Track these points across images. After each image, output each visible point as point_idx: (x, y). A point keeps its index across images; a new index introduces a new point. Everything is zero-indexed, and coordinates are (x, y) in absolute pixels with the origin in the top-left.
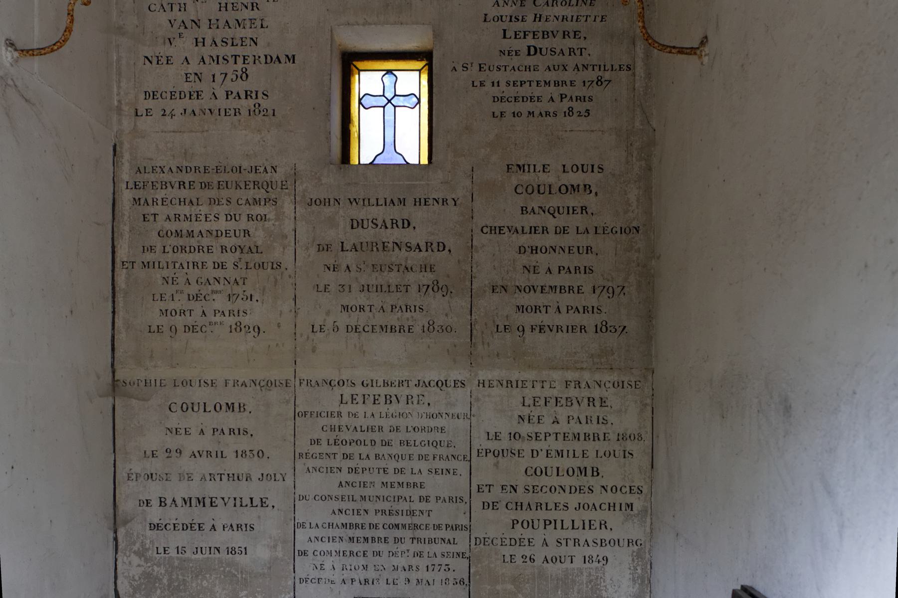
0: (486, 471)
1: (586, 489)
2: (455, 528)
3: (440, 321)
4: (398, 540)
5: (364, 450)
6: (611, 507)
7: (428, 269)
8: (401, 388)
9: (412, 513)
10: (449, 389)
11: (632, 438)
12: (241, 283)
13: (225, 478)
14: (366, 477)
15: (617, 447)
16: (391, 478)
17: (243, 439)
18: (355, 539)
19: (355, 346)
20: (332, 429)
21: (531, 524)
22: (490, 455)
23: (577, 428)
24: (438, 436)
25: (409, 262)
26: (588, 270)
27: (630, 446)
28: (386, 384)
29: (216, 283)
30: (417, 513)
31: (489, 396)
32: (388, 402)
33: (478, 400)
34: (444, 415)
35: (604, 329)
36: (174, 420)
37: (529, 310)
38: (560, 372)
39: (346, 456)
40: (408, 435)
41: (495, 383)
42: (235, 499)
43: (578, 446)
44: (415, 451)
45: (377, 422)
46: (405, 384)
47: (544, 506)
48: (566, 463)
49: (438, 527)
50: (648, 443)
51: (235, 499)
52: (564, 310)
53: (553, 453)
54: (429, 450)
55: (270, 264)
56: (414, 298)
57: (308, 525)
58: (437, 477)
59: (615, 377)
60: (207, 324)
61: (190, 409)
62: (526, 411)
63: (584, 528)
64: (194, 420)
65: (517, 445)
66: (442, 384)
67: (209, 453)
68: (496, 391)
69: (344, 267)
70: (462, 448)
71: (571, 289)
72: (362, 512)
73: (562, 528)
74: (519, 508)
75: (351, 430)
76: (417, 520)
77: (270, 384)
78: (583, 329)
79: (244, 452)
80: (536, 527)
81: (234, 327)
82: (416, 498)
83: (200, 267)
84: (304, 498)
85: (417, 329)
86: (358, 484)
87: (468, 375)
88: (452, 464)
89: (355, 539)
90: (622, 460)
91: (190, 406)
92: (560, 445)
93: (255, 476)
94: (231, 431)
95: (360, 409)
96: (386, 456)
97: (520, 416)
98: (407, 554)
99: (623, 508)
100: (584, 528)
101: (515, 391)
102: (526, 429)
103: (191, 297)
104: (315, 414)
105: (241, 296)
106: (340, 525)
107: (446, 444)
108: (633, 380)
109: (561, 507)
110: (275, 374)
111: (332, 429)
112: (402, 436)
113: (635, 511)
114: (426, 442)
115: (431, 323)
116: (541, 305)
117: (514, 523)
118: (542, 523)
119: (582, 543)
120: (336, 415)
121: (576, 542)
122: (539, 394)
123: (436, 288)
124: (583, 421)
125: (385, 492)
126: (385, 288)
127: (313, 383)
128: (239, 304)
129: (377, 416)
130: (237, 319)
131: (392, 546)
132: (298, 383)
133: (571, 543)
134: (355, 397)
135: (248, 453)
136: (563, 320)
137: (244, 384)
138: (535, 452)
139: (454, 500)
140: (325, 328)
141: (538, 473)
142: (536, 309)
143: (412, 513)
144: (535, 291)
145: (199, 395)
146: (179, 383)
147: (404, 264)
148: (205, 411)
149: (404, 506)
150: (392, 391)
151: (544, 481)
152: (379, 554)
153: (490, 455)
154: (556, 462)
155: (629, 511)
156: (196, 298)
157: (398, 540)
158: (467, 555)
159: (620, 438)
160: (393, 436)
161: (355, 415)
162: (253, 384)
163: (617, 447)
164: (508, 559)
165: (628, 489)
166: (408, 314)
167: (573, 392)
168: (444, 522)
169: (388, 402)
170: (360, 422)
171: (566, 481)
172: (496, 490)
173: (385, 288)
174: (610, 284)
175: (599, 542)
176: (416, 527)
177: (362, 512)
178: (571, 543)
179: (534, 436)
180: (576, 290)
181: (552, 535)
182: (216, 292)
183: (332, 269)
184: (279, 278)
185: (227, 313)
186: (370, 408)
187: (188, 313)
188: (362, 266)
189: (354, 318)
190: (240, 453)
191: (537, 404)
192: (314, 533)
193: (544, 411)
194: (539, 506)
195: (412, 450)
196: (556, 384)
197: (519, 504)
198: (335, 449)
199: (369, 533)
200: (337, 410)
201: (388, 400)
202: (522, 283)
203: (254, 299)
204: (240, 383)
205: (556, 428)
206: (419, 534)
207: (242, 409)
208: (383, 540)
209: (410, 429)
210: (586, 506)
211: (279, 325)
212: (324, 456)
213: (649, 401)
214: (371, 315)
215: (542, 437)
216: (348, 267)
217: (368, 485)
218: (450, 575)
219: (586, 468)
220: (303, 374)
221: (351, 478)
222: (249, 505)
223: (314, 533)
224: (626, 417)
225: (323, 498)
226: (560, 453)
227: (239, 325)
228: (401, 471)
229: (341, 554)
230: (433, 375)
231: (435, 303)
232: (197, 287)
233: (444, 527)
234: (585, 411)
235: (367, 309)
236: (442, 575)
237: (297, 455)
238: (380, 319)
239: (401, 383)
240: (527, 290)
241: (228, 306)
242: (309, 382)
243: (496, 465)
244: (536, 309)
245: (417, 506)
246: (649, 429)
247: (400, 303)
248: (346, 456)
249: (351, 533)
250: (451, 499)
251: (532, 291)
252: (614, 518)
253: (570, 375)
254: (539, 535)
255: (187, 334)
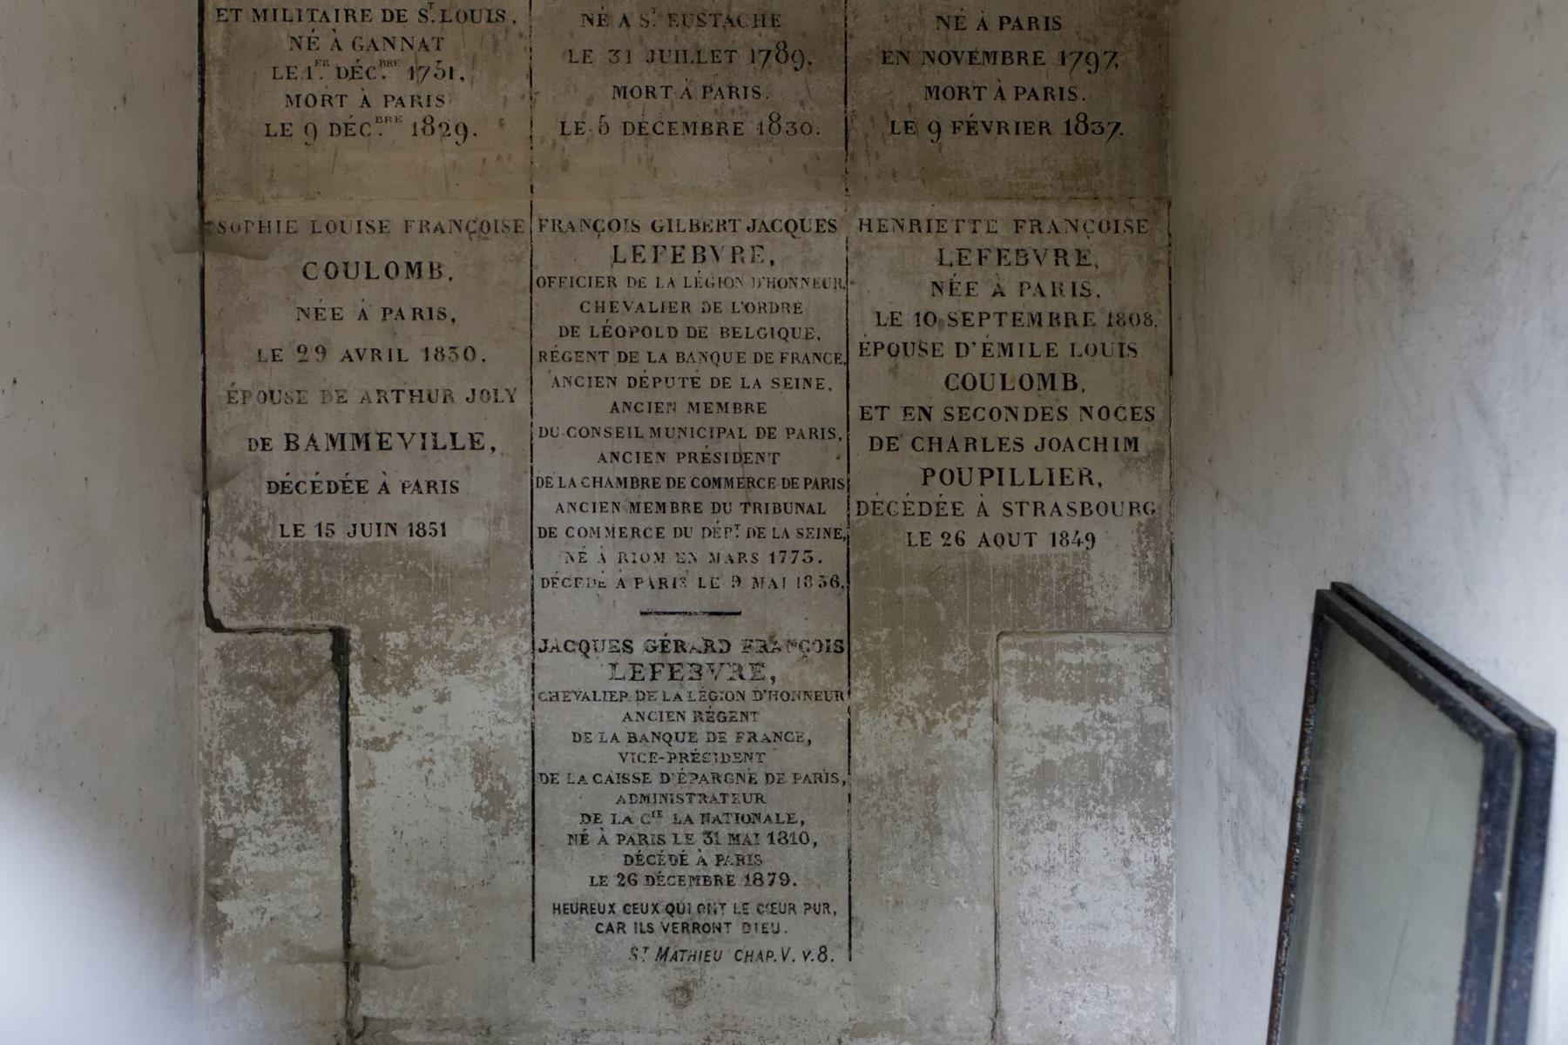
0: (873, 381)
1: (1055, 414)
2: (822, 484)
3: (791, 113)
4: (718, 508)
5: (656, 346)
6: (1100, 444)
7: (768, 23)
8: (722, 234)
9: (743, 458)
10: (808, 236)
11: (1135, 321)
12: (432, 46)
13: (405, 397)
14: (661, 394)
15: (1109, 338)
16: (705, 395)
17: (439, 326)
18: (642, 507)
19: (639, 160)
20: (599, 308)
21: (957, 477)
22: (883, 353)
23: (1036, 305)
24: (790, 320)
25: (734, 9)
26: (1051, 24)
27: (1130, 335)
28: (694, 226)
29: (388, 46)
30: (753, 458)
31: (879, 247)
32: (699, 259)
33: (859, 254)
34: (799, 282)
35: (1081, 128)
36: (314, 293)
37: (949, 95)
38: (1006, 205)
39: (624, 357)
40: (735, 317)
41: (890, 225)
42: (423, 435)
43: (1040, 336)
44: (749, 347)
45: (678, 295)
46: (729, 226)
47: (979, 445)
48: (1019, 366)
49: (791, 483)
50: (1163, 330)
51: (423, 435)
52: (1010, 94)
53: (996, 349)
54: (775, 346)
55: (485, 14)
56: (744, 72)
57: (556, 482)
58: (788, 392)
59: (1101, 213)
60: (373, 122)
61: (341, 274)
62: (946, 274)
63: (1051, 484)
64: (350, 295)
65: (930, 335)
66: (794, 227)
67: (377, 354)
68: (890, 239)
69: (618, 18)
70: (832, 342)
71: (1022, 57)
72: (654, 457)
73: (1013, 483)
74: (935, 448)
75: (633, 309)
76: (752, 471)
77: (487, 228)
78: (1044, 127)
79: (439, 351)
80: (965, 481)
81: (420, 125)
82: (750, 431)
83: (359, 17)
84: (549, 432)
85: (750, 128)
86: (646, 407)
87: (841, 210)
88: (815, 370)
89: (642, 507)
90: (1118, 360)
91: (341, 268)
92: (1006, 334)
93: (461, 393)
94: (417, 313)
95: (648, 271)
96: (696, 356)
97: (934, 283)
98: (734, 532)
99: (1121, 447)
100: (1051, 484)
101: (927, 239)
102: (944, 305)
103: (343, 73)
104: (568, 282)
105: (433, 70)
106: (614, 481)
107: (803, 334)
108: (1135, 218)
109: (1011, 445)
110: (495, 211)
111: (599, 308)
112: (727, 320)
113: (1142, 452)
114: (768, 331)
115: (774, 117)
116: (970, 85)
117: (927, 474)
118: (976, 473)
119: (1048, 509)
120: (605, 282)
121: (1038, 508)
122: (967, 244)
123: (782, 56)
124: (1048, 290)
125: (695, 421)
126: (692, 56)
127: (564, 226)
128: (431, 86)
129: (679, 283)
130: (425, 111)
131: (707, 518)
132: (536, 226)
133: (1029, 509)
134: (639, 249)
135: (447, 352)
136: (1011, 111)
137: (439, 229)
138: (963, 348)
139: (819, 434)
140: (585, 128)
141: (969, 384)
142: (961, 93)
143: (743, 458)
144: (959, 61)
145: (358, 247)
146: (320, 226)
147: (724, 13)
148: (368, 277)
149: (729, 445)
150: (707, 239)
151: (979, 398)
152: (684, 532)
153: (883, 353)
154: (997, 365)
155: (1131, 451)
156: (352, 73)
157: (718, 508)
158: (843, 533)
159: (1114, 321)
160: (706, 320)
161: (639, 283)
162: (455, 229)
163: (1109, 338)
164: (916, 540)
165: (1128, 413)
166: (734, 102)
167: (1029, 241)
168: (801, 473)
169: (699, 259)
170: (649, 294)
171: (1018, 399)
172: (895, 415)
173: (692, 56)
174: (1092, 49)
175: (1078, 507)
176: (752, 483)
177: (654, 457)
178: (1029, 509)
179: (960, 318)
180: (1031, 59)
181: (995, 495)
182: (389, 63)
183: (596, 22)
184: (501, 37)
185: (408, 102)
186: (666, 270)
187: (336, 102)
188: (650, 17)
189: (634, 110)
190: (432, 353)
191: (964, 261)
192: (567, 496)
193: (978, 274)
194: (971, 443)
195: (741, 344)
196: (998, 226)
197: (935, 440)
198: (603, 344)
199: (665, 495)
200: (607, 273)
201: (699, 255)
202: (936, 47)
203: (457, 75)
204: (432, 227)
205: (999, 304)
206: (757, 495)
207: (436, 273)
208: (692, 508)
209: (739, 307)
210: (1055, 443)
211: (501, 123)
212: (585, 356)
213: (1162, 255)
214: (667, 103)
215: (975, 320)
216: (625, 18)
217: (664, 408)
218: (812, 569)
219: (1053, 375)
220: (546, 209)
221: (633, 396)
222: (450, 446)
223: (567, 496)
224: (1123, 284)
225: (584, 432)
226: (1006, 349)
227: (429, 121)
228: (723, 383)
229: (617, 533)
230: (779, 211)
231: (783, 83)
232: (355, 55)
233: (801, 483)
234: (1050, 272)
235: (660, 93)
236: (800, 569)
237: (536, 356)
238: (682, 111)
239: (721, 226)
240: (945, 59)
241: (409, 89)
242: (556, 225)
243: (894, 371)
244: (961, 93)
245: (753, 445)
246: (1164, 306)
247: (720, 82)
248: (624, 357)
249: (634, 495)
250: (813, 432)
251: (954, 61)
252: (1104, 465)
253: (1023, 210)
254: (971, 496)
255: (334, 139)
